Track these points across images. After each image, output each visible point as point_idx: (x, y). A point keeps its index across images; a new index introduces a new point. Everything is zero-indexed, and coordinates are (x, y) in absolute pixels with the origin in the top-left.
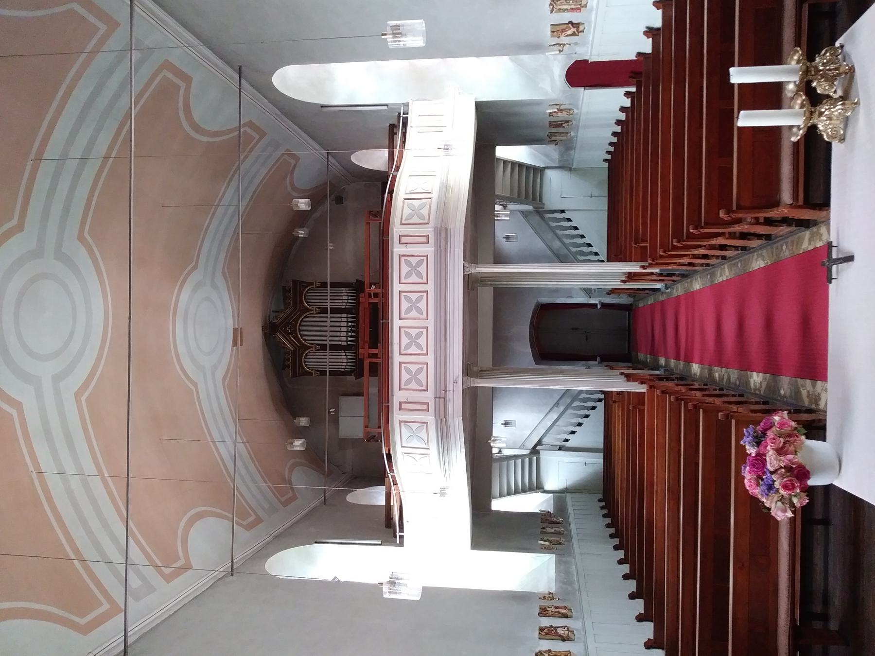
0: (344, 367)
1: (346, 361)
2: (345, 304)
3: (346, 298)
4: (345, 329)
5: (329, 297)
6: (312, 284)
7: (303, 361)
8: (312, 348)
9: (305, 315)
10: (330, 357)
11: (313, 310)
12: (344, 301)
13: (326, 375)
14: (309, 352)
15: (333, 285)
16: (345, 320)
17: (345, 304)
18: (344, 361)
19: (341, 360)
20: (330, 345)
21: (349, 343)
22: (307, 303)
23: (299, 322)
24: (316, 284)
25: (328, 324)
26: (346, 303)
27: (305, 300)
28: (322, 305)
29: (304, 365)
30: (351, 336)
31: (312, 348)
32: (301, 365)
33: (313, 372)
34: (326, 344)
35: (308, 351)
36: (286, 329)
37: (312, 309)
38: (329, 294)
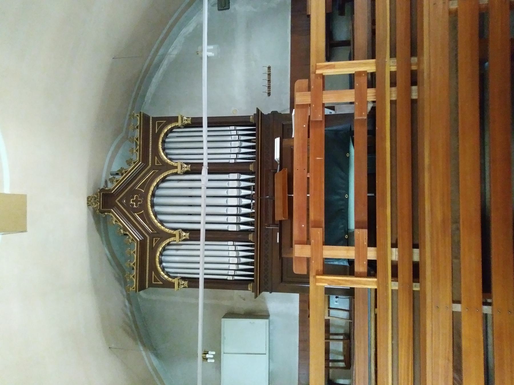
0: (232, 273)
1: (235, 260)
2: (234, 156)
3: (237, 144)
4: (234, 201)
5: (205, 145)
6: (175, 119)
7: (157, 260)
8: (174, 236)
9: (162, 176)
10: (207, 253)
11: (176, 167)
12: (234, 144)
13: (198, 287)
14: (169, 244)
15: (214, 122)
16: (235, 184)
17: (234, 156)
18: (232, 260)
19: (226, 260)
20: (207, 231)
21: (243, 227)
22: (166, 155)
23: (152, 188)
24: (182, 119)
25: (201, 192)
26: (237, 154)
27: (164, 149)
28: (194, 159)
29: (159, 268)
30: (247, 206)
31: (174, 236)
32: (153, 268)
33: (176, 281)
34: (199, 231)
35: (168, 241)
36: (128, 201)
37: (176, 165)
38: (205, 139)
